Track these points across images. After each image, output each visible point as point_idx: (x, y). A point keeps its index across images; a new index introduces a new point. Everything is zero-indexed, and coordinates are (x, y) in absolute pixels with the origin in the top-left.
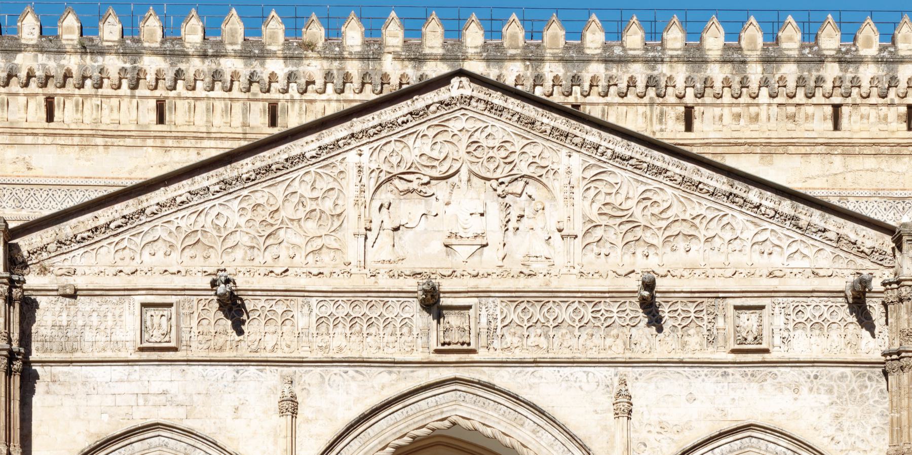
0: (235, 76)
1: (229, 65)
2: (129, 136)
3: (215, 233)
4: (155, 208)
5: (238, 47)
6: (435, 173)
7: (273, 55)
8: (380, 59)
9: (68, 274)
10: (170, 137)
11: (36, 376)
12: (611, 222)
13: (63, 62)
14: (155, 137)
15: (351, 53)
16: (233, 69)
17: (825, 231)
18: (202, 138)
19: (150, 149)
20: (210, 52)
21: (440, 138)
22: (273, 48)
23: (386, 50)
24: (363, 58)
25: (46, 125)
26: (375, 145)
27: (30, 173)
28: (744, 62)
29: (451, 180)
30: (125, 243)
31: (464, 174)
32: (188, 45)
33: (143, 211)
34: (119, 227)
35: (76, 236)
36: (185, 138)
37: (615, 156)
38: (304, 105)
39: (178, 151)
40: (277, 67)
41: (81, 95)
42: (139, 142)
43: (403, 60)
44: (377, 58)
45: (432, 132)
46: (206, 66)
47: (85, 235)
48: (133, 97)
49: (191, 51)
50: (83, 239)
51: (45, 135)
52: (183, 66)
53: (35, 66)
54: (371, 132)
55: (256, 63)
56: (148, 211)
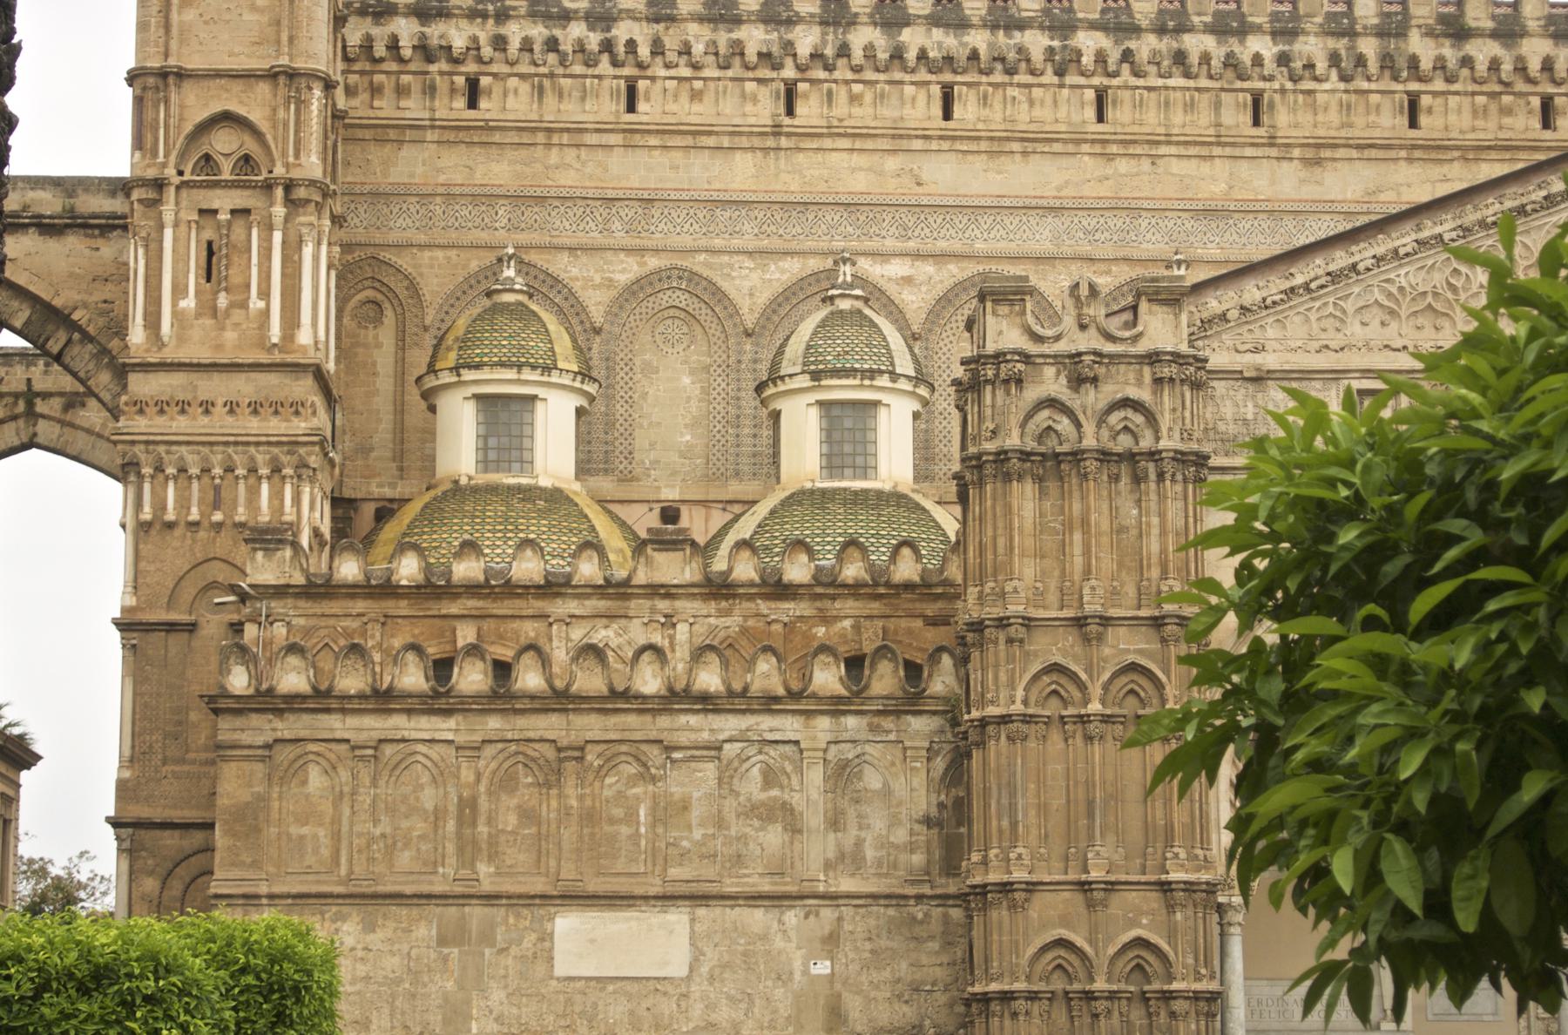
0: (1206, 58)
1: (1196, 44)
2: (1057, 140)
3: (1450, 295)
4: (1369, 262)
5: (1208, 19)
7: (1258, 29)
8: (1405, 35)
9: (1256, 350)
10: (1115, 142)
13: (966, 39)
14: (1093, 141)
15: (1365, 27)
16: (1202, 48)
18: (1158, 143)
19: (1086, 158)
20: (1171, 24)
22: (1258, 20)
23: (1414, 22)
24: (1381, 33)
25: (944, 124)
27: (920, 190)
30: (1331, 309)
32: (1138, 16)
33: (1354, 267)
34: (1322, 287)
35: (1264, 300)
36: (1135, 142)
38: (1301, 97)
39: (1124, 161)
40: (1262, 46)
41: (990, 84)
42: (1071, 148)
43: (1437, 36)
44: (1401, 33)
46: (1165, 45)
47: (1277, 298)
48: (1062, 86)
49: (1144, 23)
50: (1274, 303)
51: (941, 138)
52: (1132, 45)
53: (928, 44)
55: (1233, 41)
56: (1361, 267)
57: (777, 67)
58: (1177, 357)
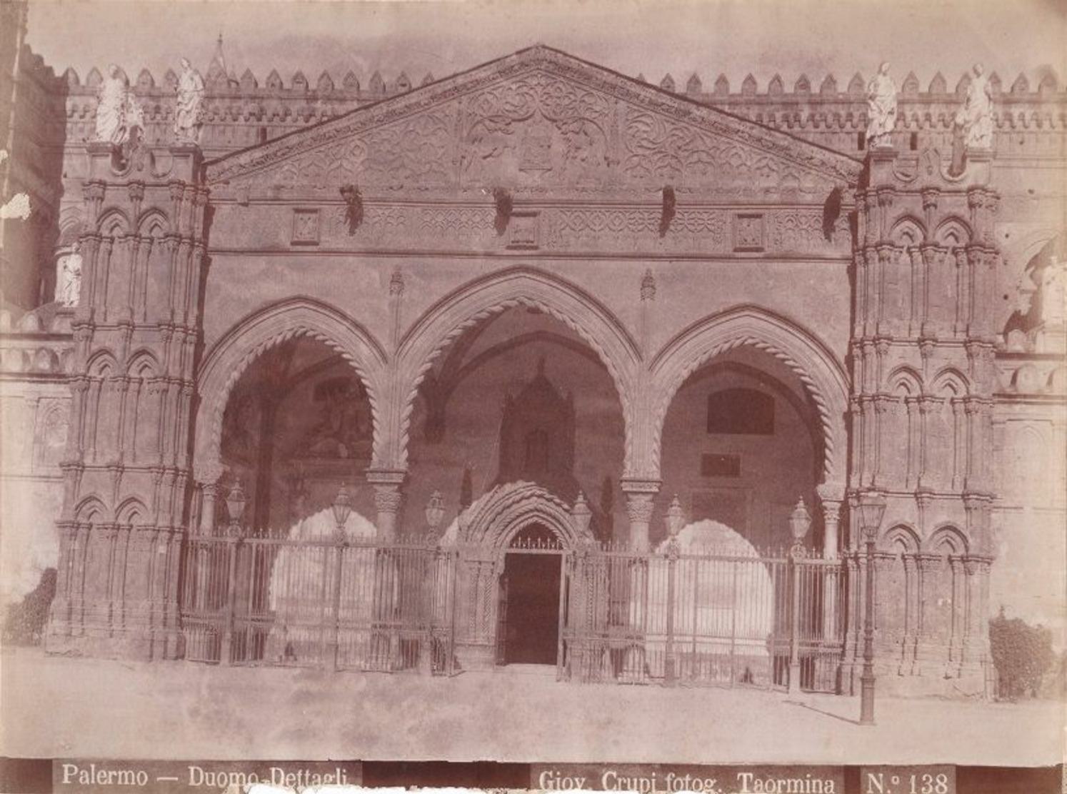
6: (516, 116)
11: (210, 260)
12: (647, 152)
17: (812, 158)
21: (520, 91)
26: (472, 95)
28: (797, 104)
29: (527, 122)
31: (538, 117)
37: (651, 102)
45: (514, 87)
54: (469, 86)
57: (259, 120)
58: (182, 185)
